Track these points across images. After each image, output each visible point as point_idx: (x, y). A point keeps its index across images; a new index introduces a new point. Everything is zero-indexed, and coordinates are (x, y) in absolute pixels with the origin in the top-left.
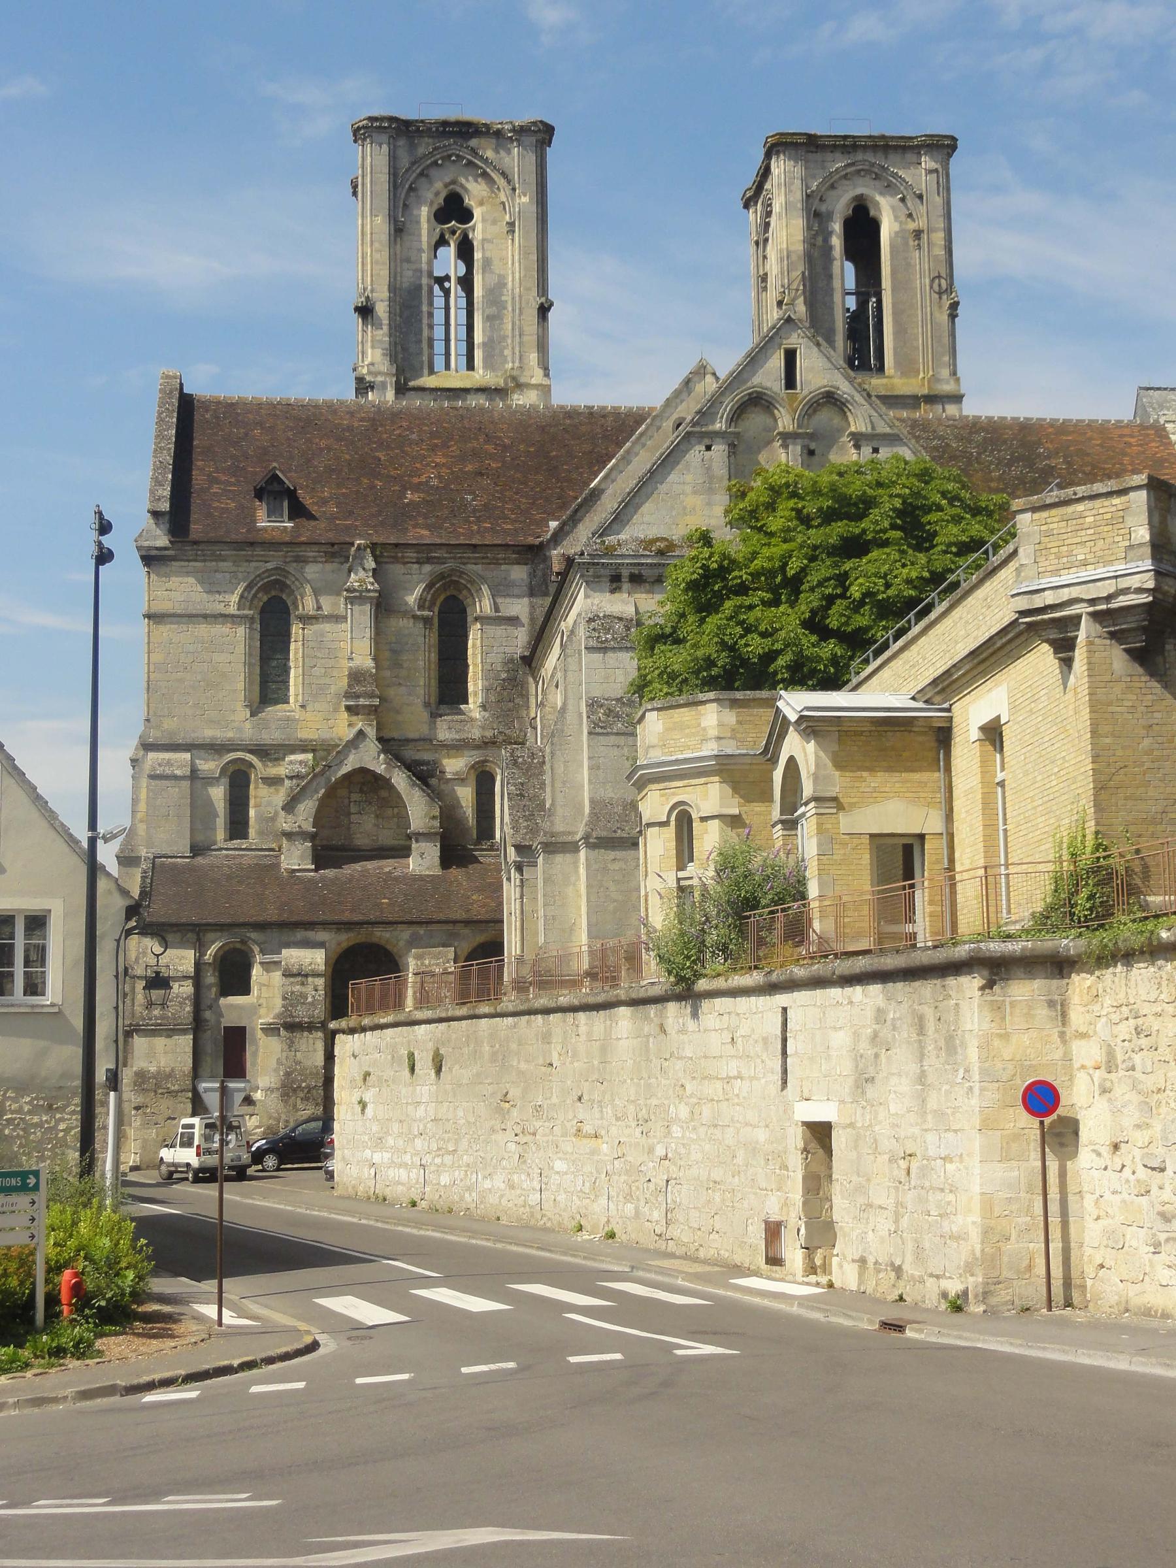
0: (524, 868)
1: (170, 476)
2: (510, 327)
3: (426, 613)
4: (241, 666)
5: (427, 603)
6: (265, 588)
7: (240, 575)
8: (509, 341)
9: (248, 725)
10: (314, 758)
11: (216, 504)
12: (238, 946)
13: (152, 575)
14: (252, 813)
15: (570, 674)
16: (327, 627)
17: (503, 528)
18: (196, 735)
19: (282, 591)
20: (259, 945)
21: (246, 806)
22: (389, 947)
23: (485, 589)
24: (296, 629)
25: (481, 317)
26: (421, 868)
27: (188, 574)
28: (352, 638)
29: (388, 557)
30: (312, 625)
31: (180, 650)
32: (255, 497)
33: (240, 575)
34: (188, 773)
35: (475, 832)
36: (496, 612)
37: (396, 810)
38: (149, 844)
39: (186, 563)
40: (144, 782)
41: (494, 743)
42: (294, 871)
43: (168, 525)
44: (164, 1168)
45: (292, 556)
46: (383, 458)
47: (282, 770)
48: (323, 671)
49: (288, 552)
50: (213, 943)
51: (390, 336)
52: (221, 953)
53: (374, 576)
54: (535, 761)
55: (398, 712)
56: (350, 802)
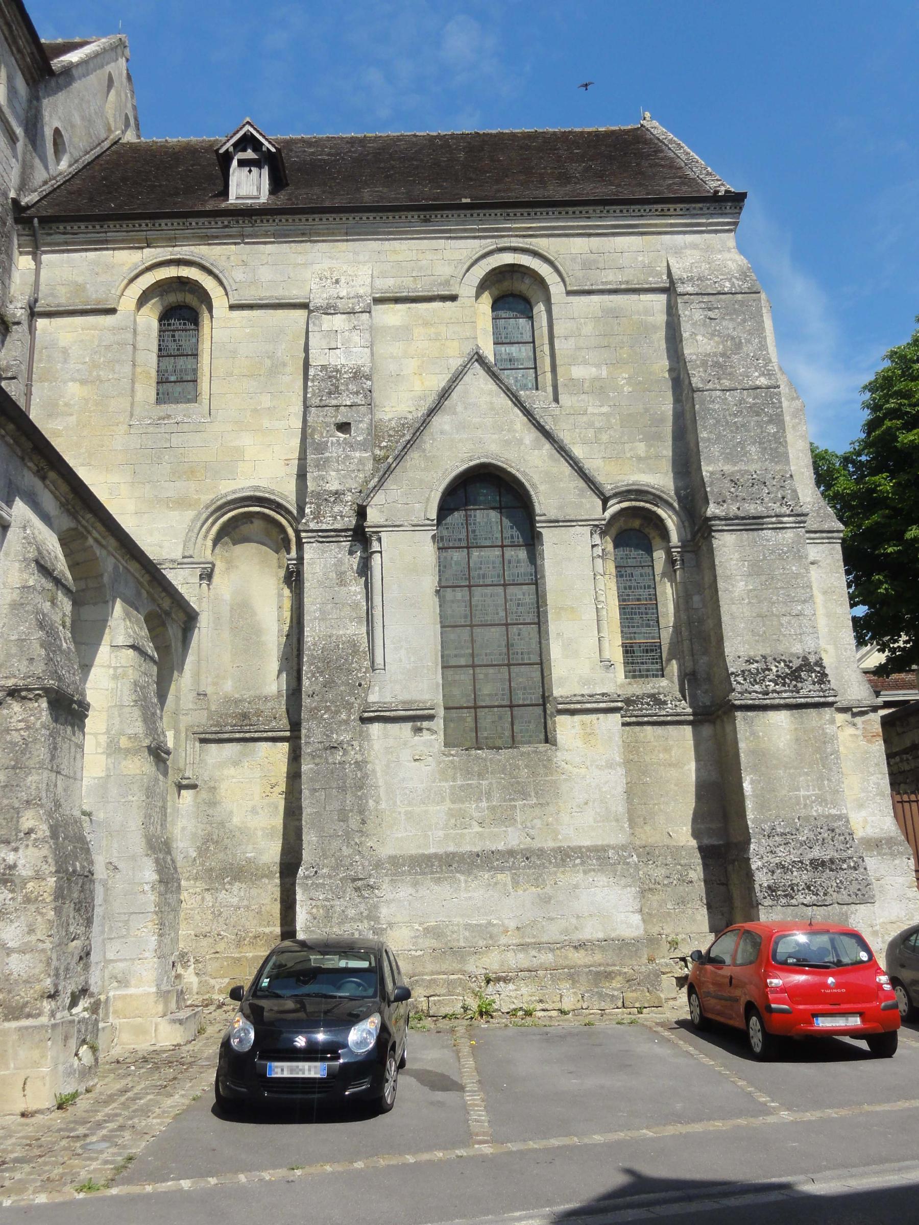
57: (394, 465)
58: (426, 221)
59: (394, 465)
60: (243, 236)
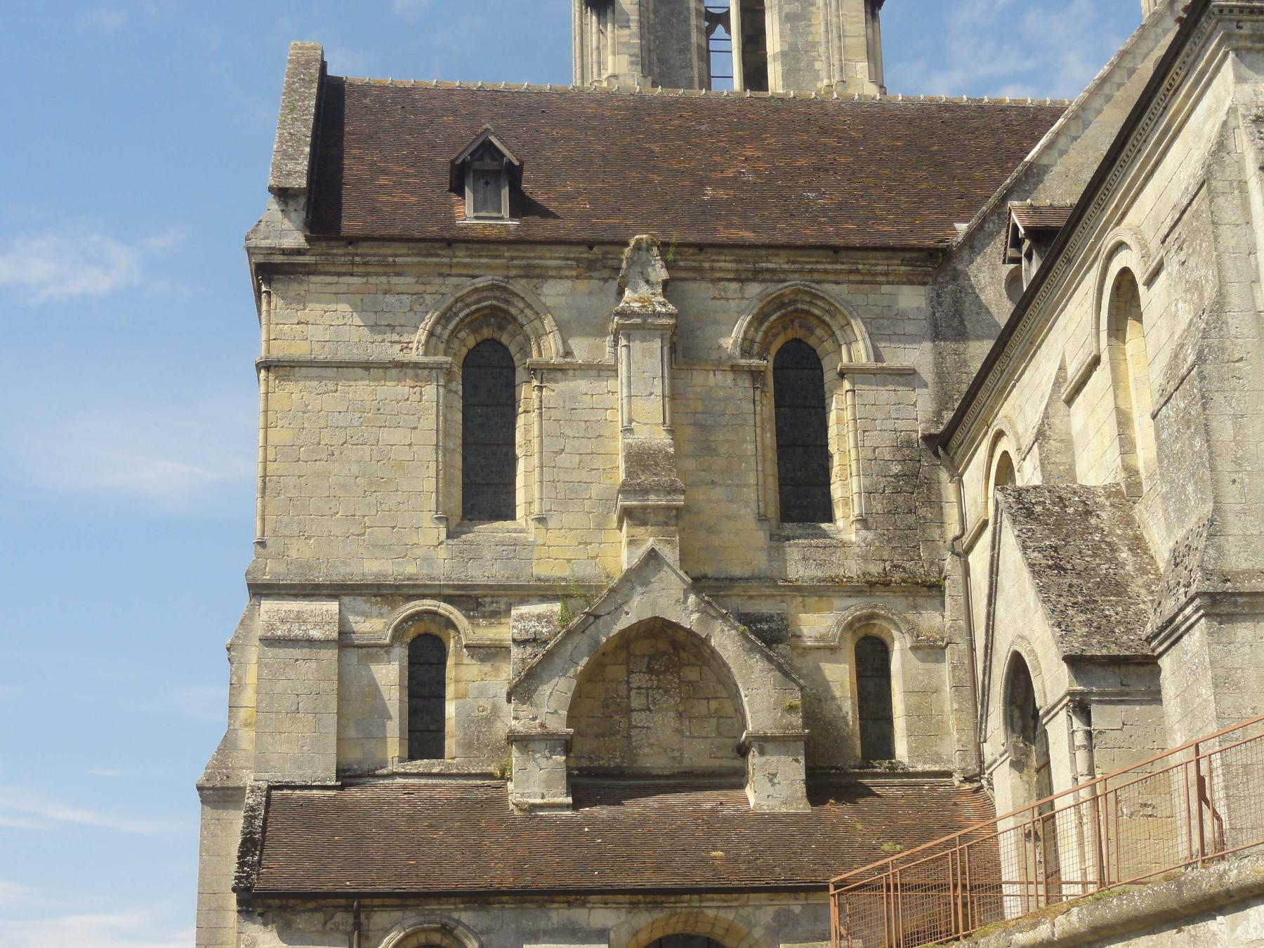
0: (1094, 709)
1: (307, 149)
2: (822, 29)
3: (755, 362)
4: (430, 453)
5: (756, 348)
6: (473, 323)
7: (428, 299)
8: (822, 49)
9: (442, 553)
10: (565, 608)
11: (385, 198)
13: (274, 298)
14: (450, 709)
15: (1225, 231)
16: (582, 385)
18: (349, 570)
19: (501, 328)
20: (477, 935)
21: (439, 698)
23: (858, 327)
24: (527, 394)
25: (776, 17)
26: (772, 802)
27: (337, 296)
28: (630, 396)
29: (686, 269)
30: (556, 381)
31: (322, 423)
32: (450, 190)
33: (428, 299)
34: (335, 635)
35: (858, 742)
36: (876, 361)
37: (714, 704)
38: (261, 764)
39: (335, 279)
40: (253, 652)
42: (534, 807)
43: (303, 214)
46: (657, 150)
47: (504, 632)
48: (577, 458)
49: (512, 258)
50: (387, 931)
51: (642, 38)
53: (665, 293)
54: (1070, 510)
55: (711, 531)
56: (630, 689)
57: (987, 682)
58: (1070, 261)
59: (987, 682)
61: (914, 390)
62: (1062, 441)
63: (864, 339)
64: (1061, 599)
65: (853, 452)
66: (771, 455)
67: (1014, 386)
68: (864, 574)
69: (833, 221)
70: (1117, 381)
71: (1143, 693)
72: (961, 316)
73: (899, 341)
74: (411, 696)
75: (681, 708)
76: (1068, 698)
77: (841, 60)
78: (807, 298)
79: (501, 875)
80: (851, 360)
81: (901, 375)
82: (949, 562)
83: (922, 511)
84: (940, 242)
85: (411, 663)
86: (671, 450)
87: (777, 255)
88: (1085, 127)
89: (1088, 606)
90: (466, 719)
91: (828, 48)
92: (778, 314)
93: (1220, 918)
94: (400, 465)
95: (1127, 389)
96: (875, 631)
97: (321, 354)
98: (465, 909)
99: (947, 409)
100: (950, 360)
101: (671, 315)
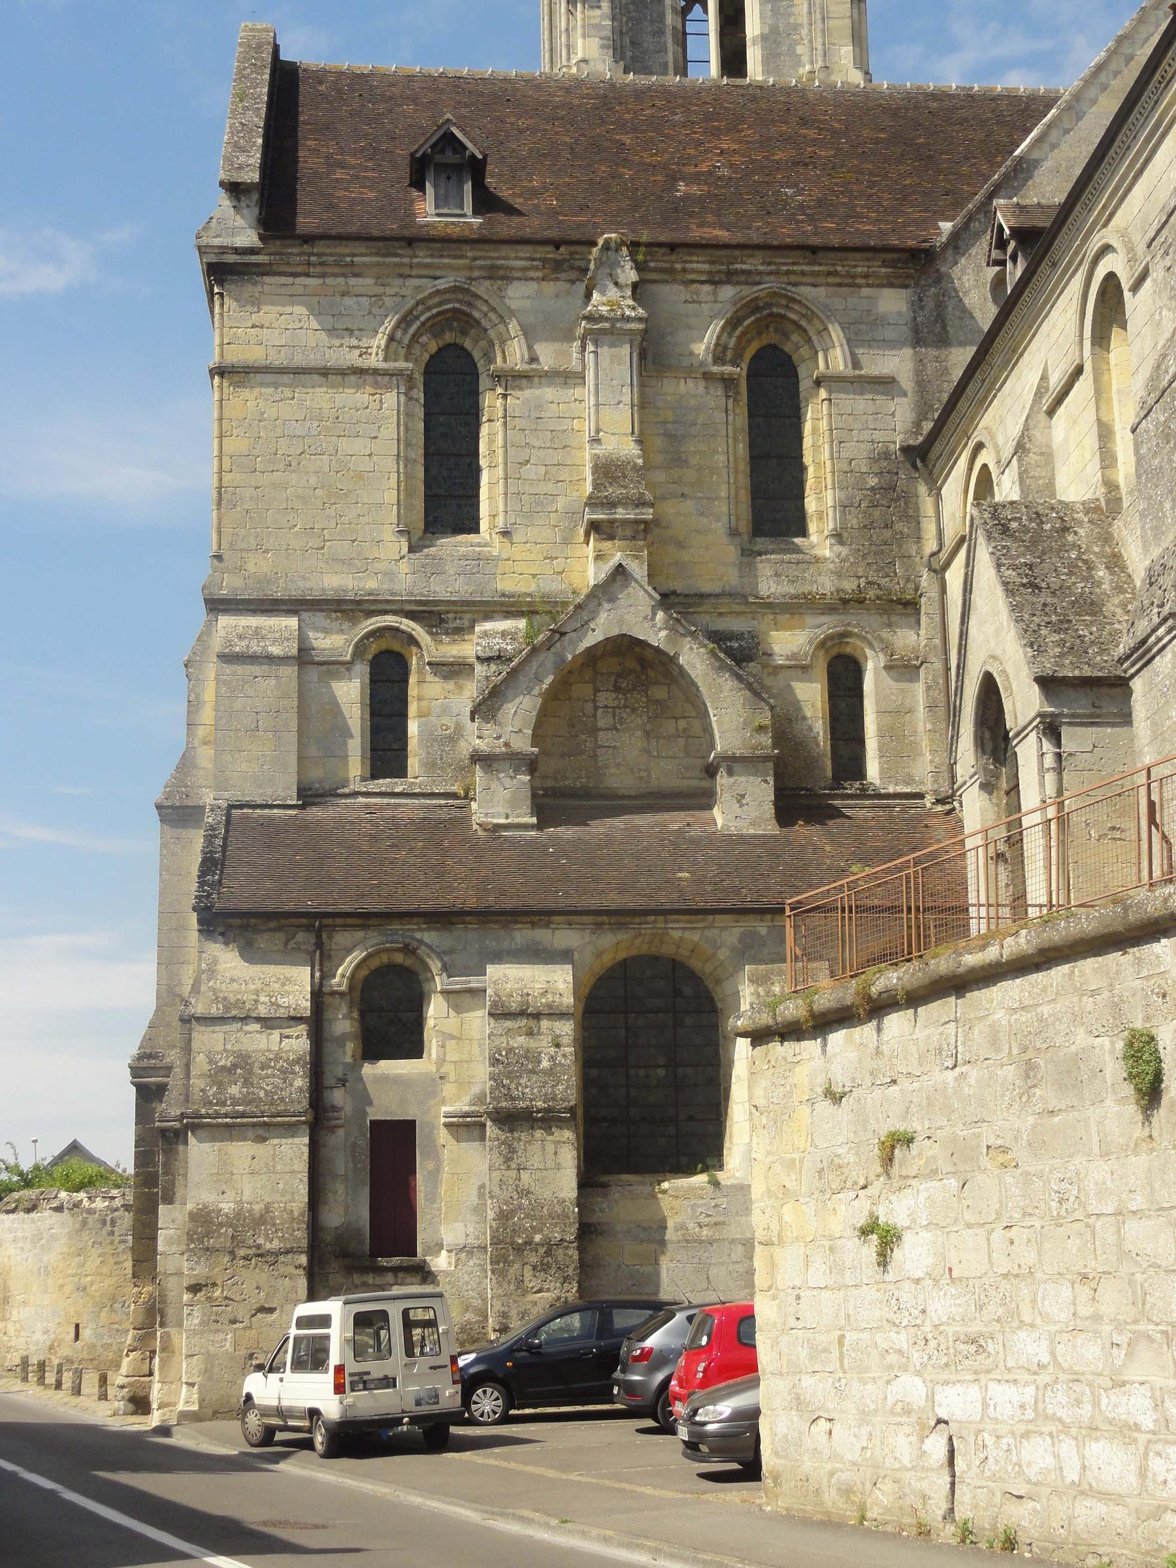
0: (1065, 731)
1: (260, 141)
2: (805, 9)
3: (728, 369)
4: (391, 464)
5: (729, 354)
6: (436, 326)
8: (804, 32)
9: (404, 567)
10: (530, 624)
11: (341, 193)
12: (399, 958)
13: (226, 299)
14: (413, 727)
16: (548, 393)
17: (857, 230)
18: (308, 584)
19: (464, 333)
20: (440, 955)
22: (695, 964)
23: (836, 333)
24: (491, 402)
26: (739, 823)
27: (292, 299)
28: (597, 405)
29: (656, 270)
30: (521, 389)
31: (279, 432)
32: (411, 185)
34: (295, 652)
35: (829, 763)
37: (682, 724)
38: (220, 784)
39: (290, 280)
40: (211, 669)
41: (861, 602)
42: (498, 827)
43: (256, 211)
44: (253, 1419)
45: (482, 268)
46: (628, 142)
49: (475, 259)
50: (349, 951)
51: (613, 19)
52: (364, 972)
53: (634, 296)
54: (1047, 527)
55: (681, 545)
56: (596, 708)
58: (1054, 265)
60: (994, 383)
61: (893, 399)
62: (1042, 454)
63: (842, 345)
64: (1035, 618)
65: (828, 463)
66: (744, 467)
67: (995, 396)
68: (838, 591)
69: (811, 219)
70: (1100, 392)
71: (1115, 715)
72: (943, 321)
73: (879, 348)
74: (372, 714)
75: (648, 727)
76: (1038, 719)
77: (824, 44)
78: (783, 302)
79: (465, 896)
80: (827, 367)
81: (880, 383)
82: (926, 579)
83: (898, 526)
84: (924, 242)
85: (373, 681)
86: (640, 462)
87: (752, 256)
88: (1079, 118)
89: (1062, 625)
90: (428, 738)
91: (810, 31)
92: (753, 318)
93: (1164, 941)
94: (360, 476)
95: (1110, 400)
96: (848, 650)
97: (278, 360)
98: (428, 929)
99: (926, 419)
100: (931, 368)
101: (640, 319)
